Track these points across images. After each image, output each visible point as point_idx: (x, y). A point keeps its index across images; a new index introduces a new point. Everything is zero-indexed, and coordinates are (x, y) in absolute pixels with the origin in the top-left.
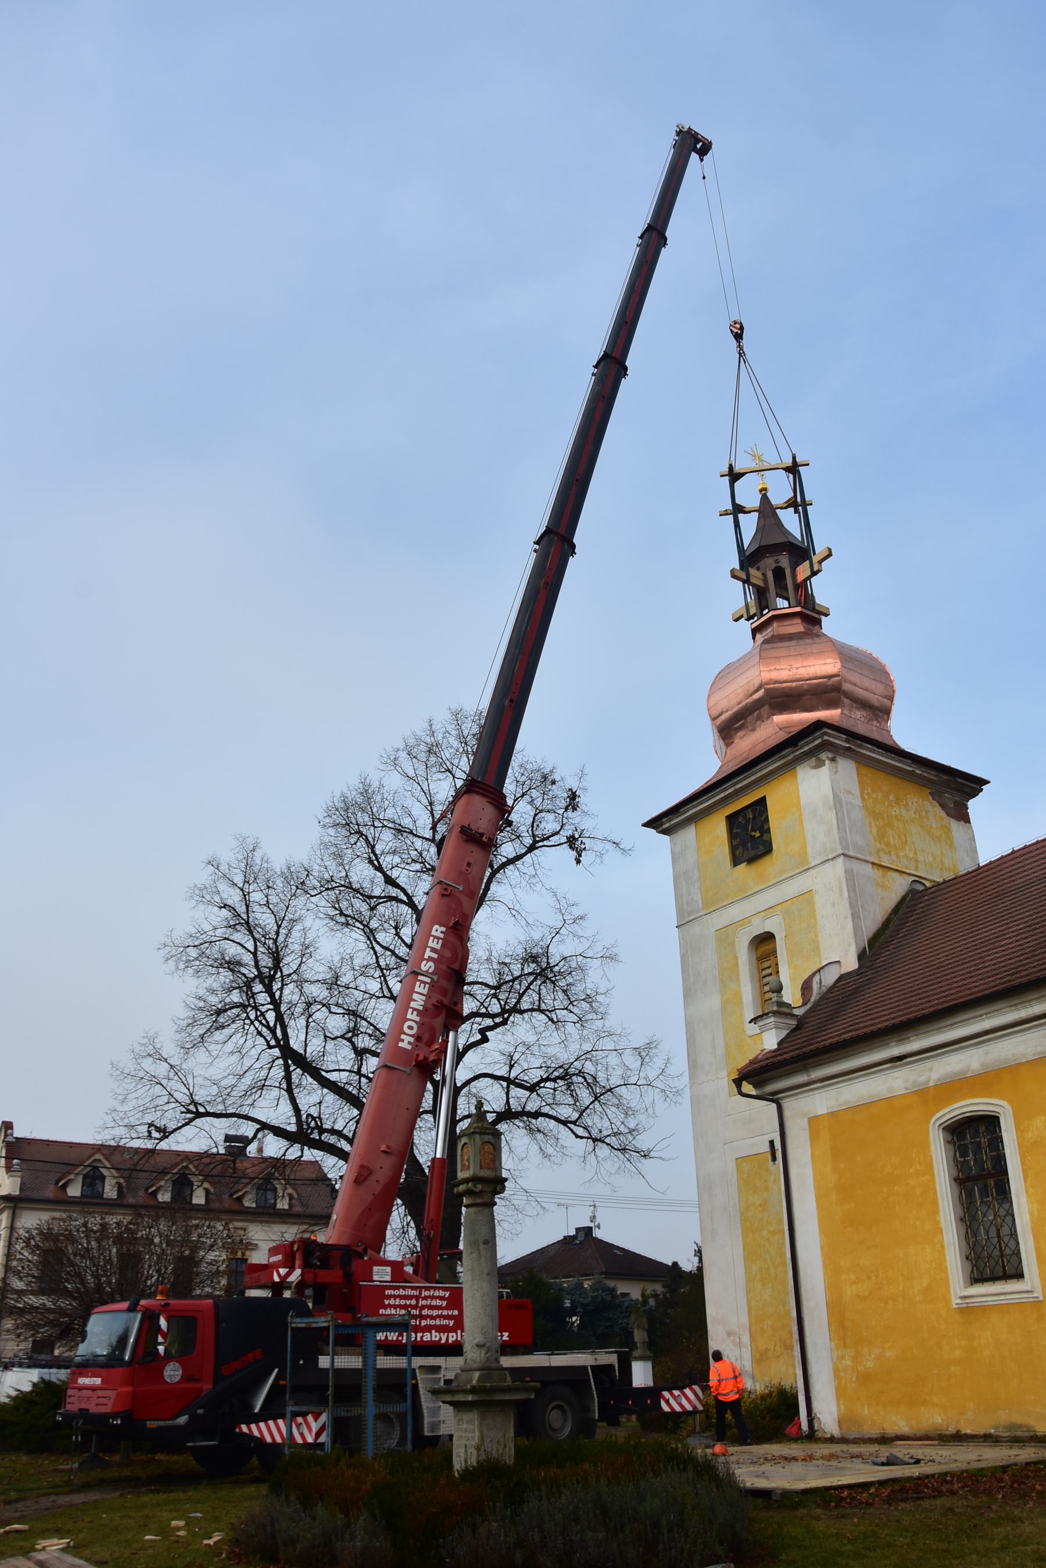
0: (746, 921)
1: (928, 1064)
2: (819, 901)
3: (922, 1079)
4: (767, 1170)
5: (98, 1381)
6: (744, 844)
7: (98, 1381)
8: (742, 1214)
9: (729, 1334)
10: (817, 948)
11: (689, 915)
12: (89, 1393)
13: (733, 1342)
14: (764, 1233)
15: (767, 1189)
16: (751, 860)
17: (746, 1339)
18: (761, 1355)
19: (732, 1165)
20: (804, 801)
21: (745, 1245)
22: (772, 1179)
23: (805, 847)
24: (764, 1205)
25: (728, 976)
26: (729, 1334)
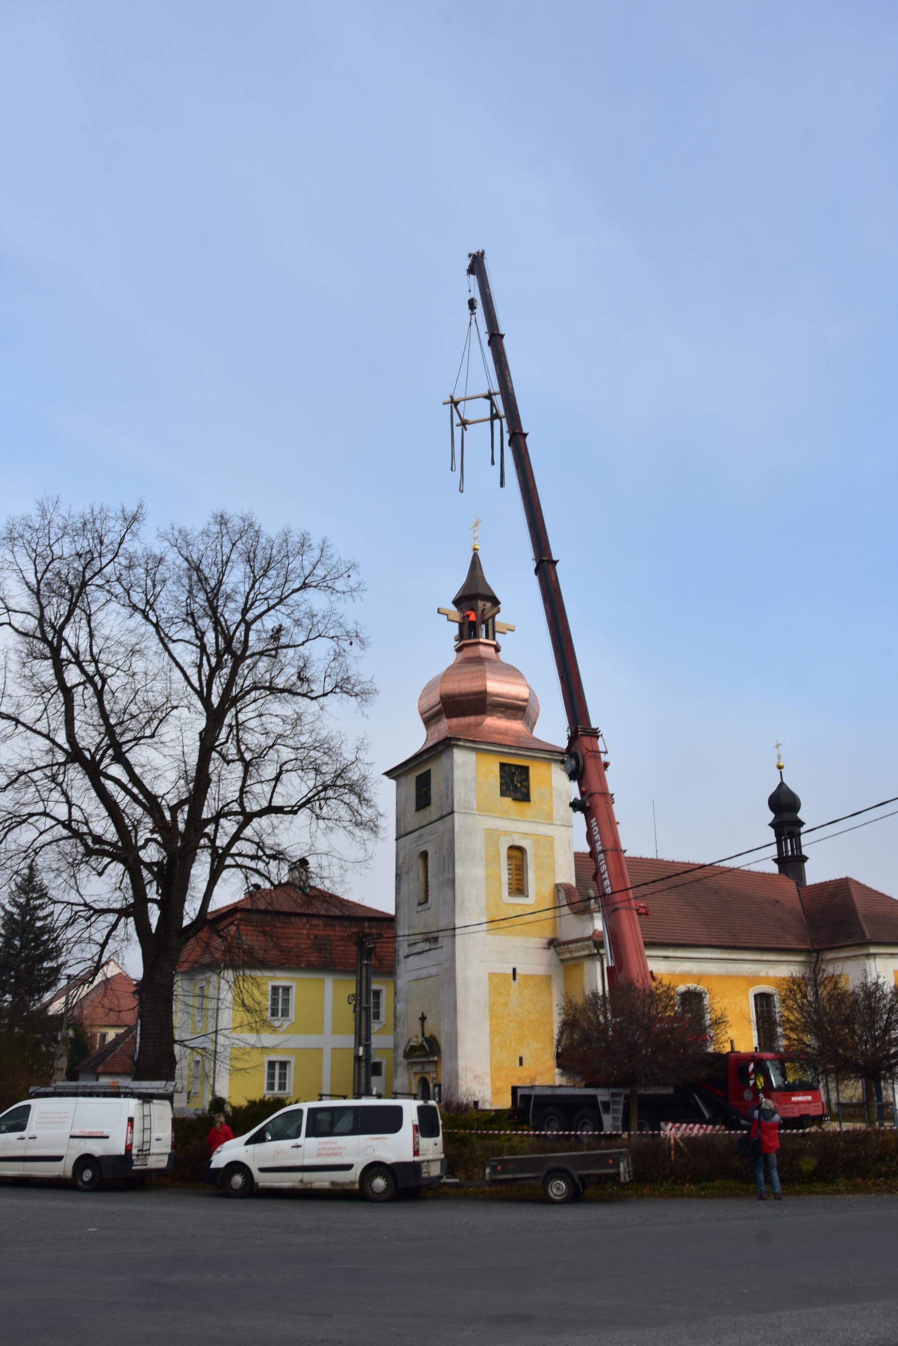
0: (506, 833)
1: (676, 963)
2: (557, 845)
3: (673, 969)
4: (510, 984)
5: (810, 1098)
6: (508, 786)
7: (810, 1098)
8: (490, 1007)
9: (475, 1077)
10: (553, 870)
11: (465, 809)
12: (807, 1105)
13: (479, 1082)
14: (505, 1020)
15: (508, 995)
16: (515, 799)
17: (488, 1081)
18: (497, 1090)
19: (486, 977)
20: (554, 784)
21: (491, 1026)
22: (512, 990)
23: (551, 811)
24: (506, 1004)
25: (491, 861)
26: (475, 1077)
